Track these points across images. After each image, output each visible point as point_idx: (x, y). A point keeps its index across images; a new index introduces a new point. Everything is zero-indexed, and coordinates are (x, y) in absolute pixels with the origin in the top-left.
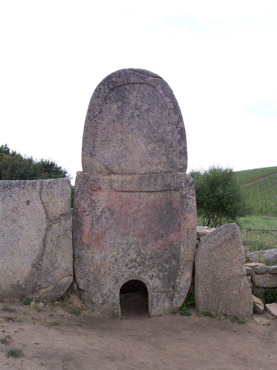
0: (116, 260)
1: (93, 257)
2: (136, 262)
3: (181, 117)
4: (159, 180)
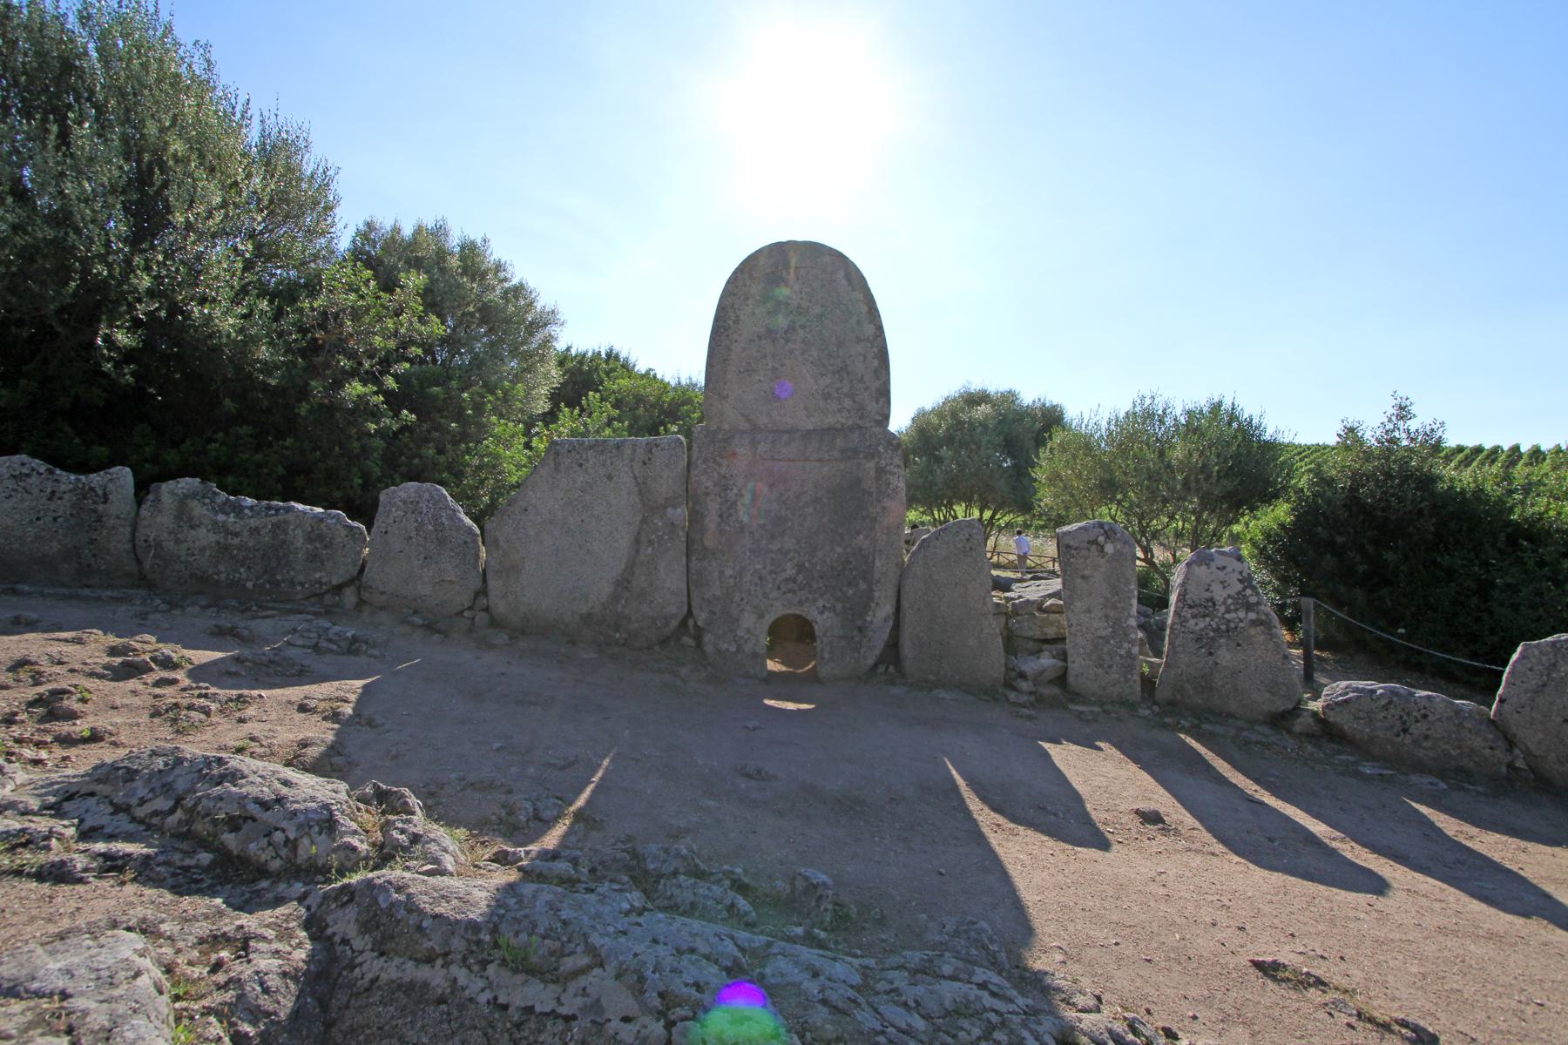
0: (761, 578)
1: (722, 573)
3: (880, 329)
4: (839, 442)
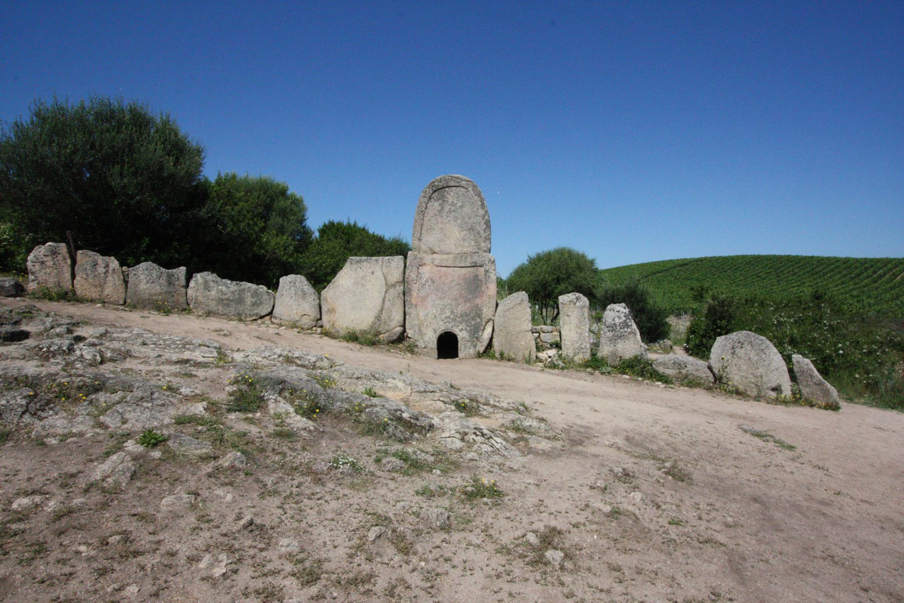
1: (418, 314)
4: (469, 259)
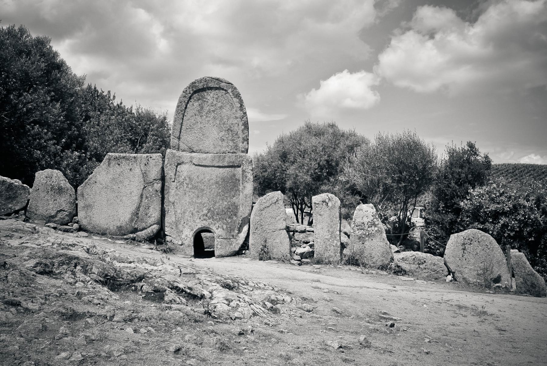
0: (192, 214)
2: (206, 216)
